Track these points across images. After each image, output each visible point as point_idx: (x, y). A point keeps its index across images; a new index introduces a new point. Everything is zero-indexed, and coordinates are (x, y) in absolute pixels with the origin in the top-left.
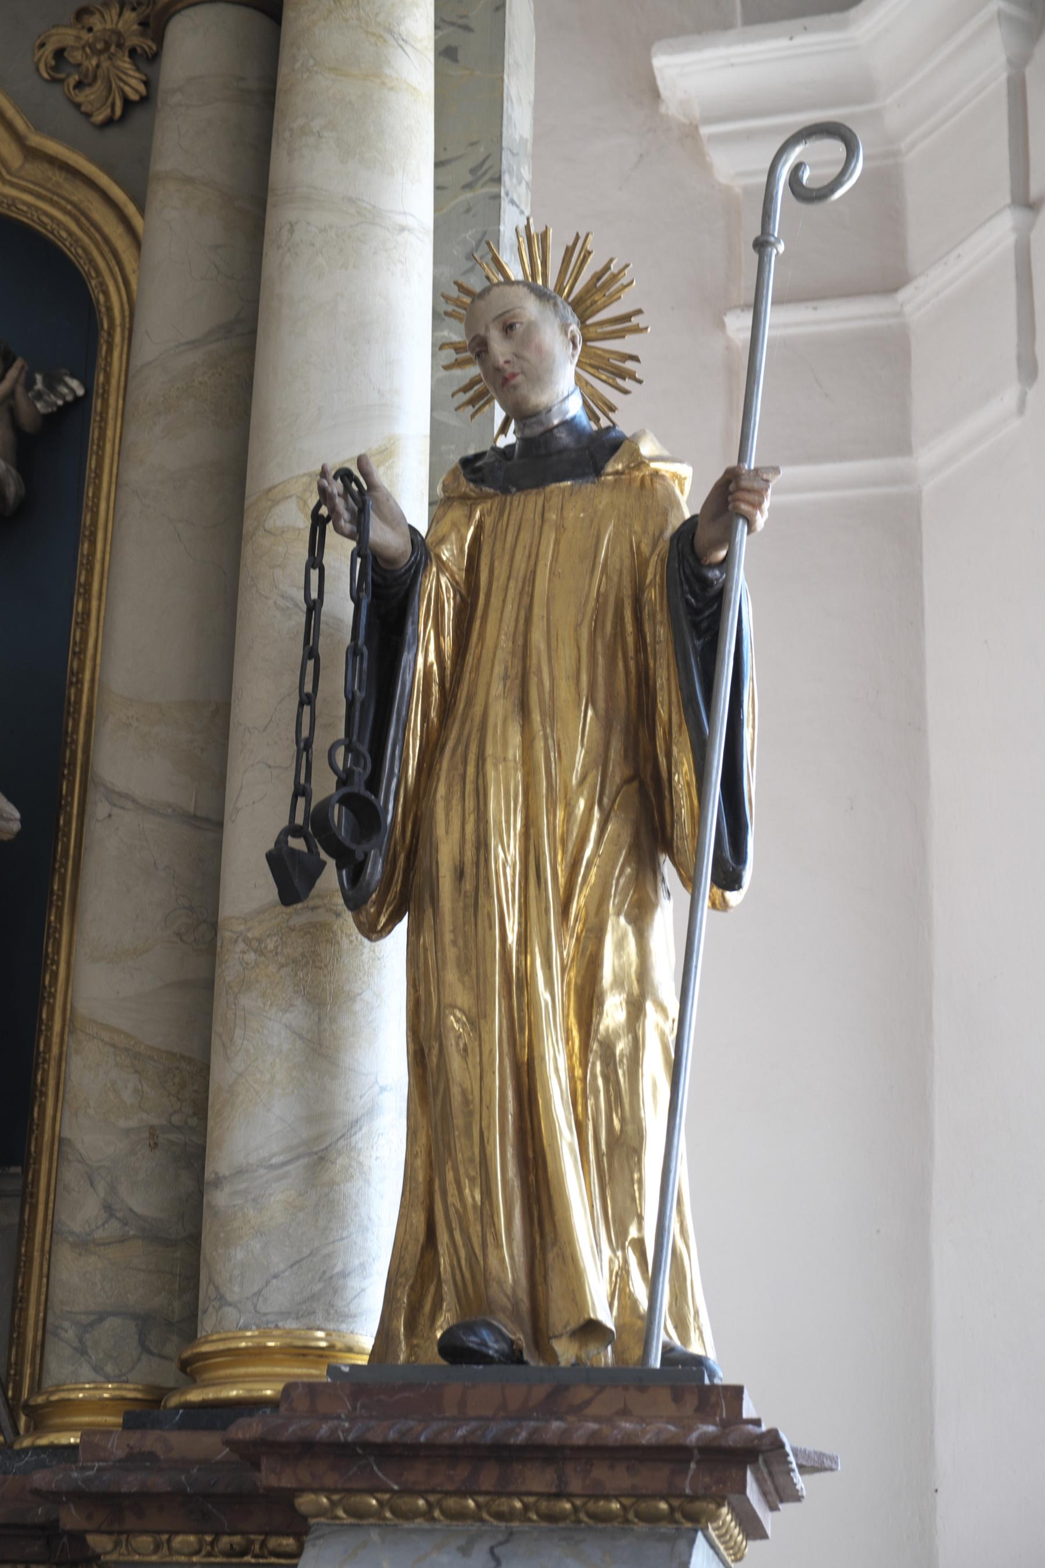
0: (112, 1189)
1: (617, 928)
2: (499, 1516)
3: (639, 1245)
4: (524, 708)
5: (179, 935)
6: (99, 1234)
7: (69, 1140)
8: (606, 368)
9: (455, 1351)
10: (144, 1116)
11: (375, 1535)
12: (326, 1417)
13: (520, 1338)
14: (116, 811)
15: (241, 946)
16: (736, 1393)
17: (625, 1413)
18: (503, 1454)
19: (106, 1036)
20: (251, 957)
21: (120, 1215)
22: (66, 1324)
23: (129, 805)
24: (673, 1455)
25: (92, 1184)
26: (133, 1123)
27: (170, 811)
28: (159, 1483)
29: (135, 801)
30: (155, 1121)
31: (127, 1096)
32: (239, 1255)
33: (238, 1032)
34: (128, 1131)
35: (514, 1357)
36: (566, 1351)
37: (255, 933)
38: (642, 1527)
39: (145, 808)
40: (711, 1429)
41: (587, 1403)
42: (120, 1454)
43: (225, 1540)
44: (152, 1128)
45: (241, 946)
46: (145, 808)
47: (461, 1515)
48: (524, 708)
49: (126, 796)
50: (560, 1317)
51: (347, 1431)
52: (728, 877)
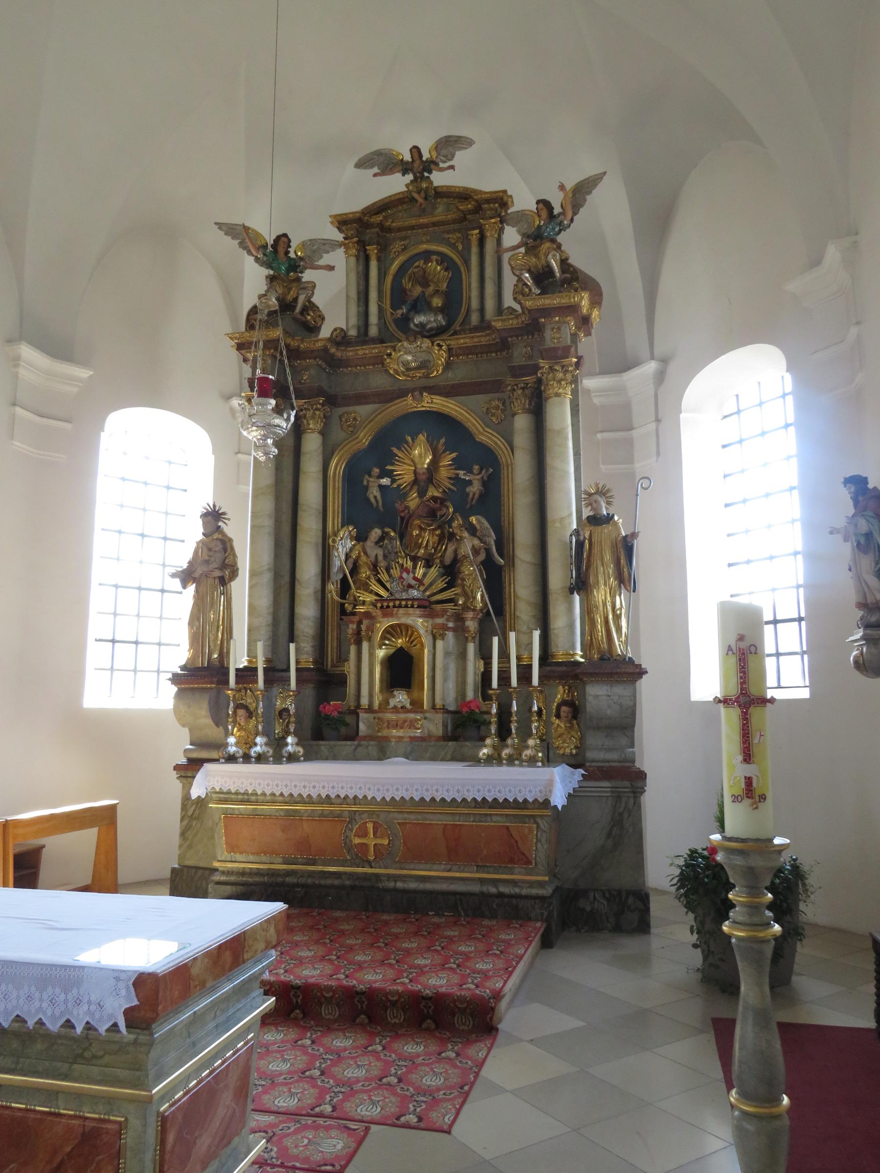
1: (618, 598)
4: (603, 564)
8: (609, 503)
18: (611, 673)
24: (633, 673)
35: (609, 659)
46: (528, 563)
48: (603, 564)
50: (614, 654)
51: (592, 671)
52: (634, 591)
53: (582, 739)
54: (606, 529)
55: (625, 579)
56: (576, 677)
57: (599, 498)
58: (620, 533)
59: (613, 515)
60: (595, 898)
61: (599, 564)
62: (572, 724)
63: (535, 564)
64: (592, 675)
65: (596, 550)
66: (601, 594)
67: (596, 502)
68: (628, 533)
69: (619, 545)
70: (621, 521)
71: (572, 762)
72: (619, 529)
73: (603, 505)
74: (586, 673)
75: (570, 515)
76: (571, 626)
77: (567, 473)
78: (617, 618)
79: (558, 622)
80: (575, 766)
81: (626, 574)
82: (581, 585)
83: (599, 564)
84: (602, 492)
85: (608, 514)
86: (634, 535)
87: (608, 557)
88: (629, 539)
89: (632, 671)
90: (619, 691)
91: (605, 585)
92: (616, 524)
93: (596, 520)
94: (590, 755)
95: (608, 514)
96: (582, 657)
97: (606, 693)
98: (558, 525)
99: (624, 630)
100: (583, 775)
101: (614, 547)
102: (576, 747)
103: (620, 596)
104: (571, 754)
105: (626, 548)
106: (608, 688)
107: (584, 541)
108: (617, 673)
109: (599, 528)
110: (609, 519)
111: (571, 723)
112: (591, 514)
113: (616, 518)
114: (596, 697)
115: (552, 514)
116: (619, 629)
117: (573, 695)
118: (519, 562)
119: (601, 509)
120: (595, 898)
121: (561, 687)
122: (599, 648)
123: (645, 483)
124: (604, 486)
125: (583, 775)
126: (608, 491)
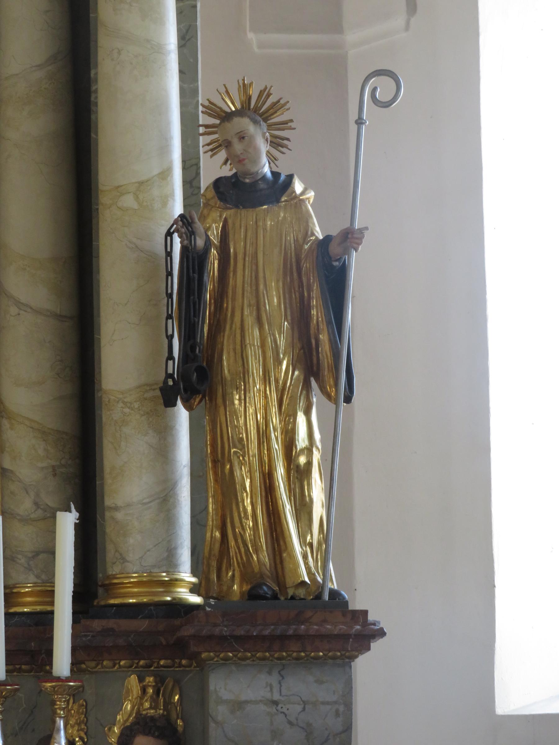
0: (37, 495)
2: (279, 659)
3: (311, 545)
5: (58, 374)
6: (33, 516)
7: (12, 472)
10: (50, 461)
11: (233, 668)
12: (215, 625)
13: (276, 588)
14: (22, 312)
15: (121, 405)
16: (365, 613)
17: (325, 621)
18: (283, 639)
19: (27, 423)
20: (127, 410)
21: (42, 507)
22: (20, 556)
23: (29, 310)
24: (344, 637)
25: (27, 493)
26: (44, 464)
27: (49, 313)
28: (121, 642)
29: (31, 308)
30: (53, 463)
31: (41, 452)
32: (131, 541)
33: (123, 444)
34: (43, 468)
35: (275, 597)
36: (291, 592)
37: (128, 399)
38: (330, 661)
39: (37, 312)
40: (358, 627)
41: (311, 617)
42: (99, 629)
43: (142, 662)
44: (53, 467)
45: (121, 405)
46: (37, 312)
47: (264, 659)
49: (27, 305)
50: (290, 581)
51: (226, 631)
54: (270, 218)
55: (322, 365)
56: (179, 648)
57: (251, 128)
58: (307, 232)
59: (290, 178)
61: (250, 320)
63: (60, 317)
64: (223, 642)
65: (239, 278)
66: (251, 409)
68: (334, 232)
70: (311, 194)
72: (303, 220)
73: (263, 147)
74: (210, 637)
75: (166, 174)
76: (166, 499)
77: (159, 49)
78: (299, 475)
79: (127, 487)
81: (325, 347)
82: (196, 378)
83: (250, 320)
84: (259, 109)
86: (350, 238)
87: (274, 300)
88: (334, 249)
89: (341, 628)
90: (302, 686)
91: (266, 379)
92: (298, 202)
93: (240, 191)
96: (194, 589)
97: (264, 693)
98: (128, 201)
99: (318, 511)
101: (293, 269)
103: (308, 413)
105: (325, 274)
106: (274, 679)
108: (298, 637)
109: (248, 216)
110: (278, 188)
112: (227, 171)
113: (298, 187)
114: (238, 706)
115: (111, 172)
116: (303, 508)
117: (168, 703)
118: (13, 310)
119: (256, 160)
121: (133, 679)
123: (384, 88)
124: (265, 94)
126: (277, 107)
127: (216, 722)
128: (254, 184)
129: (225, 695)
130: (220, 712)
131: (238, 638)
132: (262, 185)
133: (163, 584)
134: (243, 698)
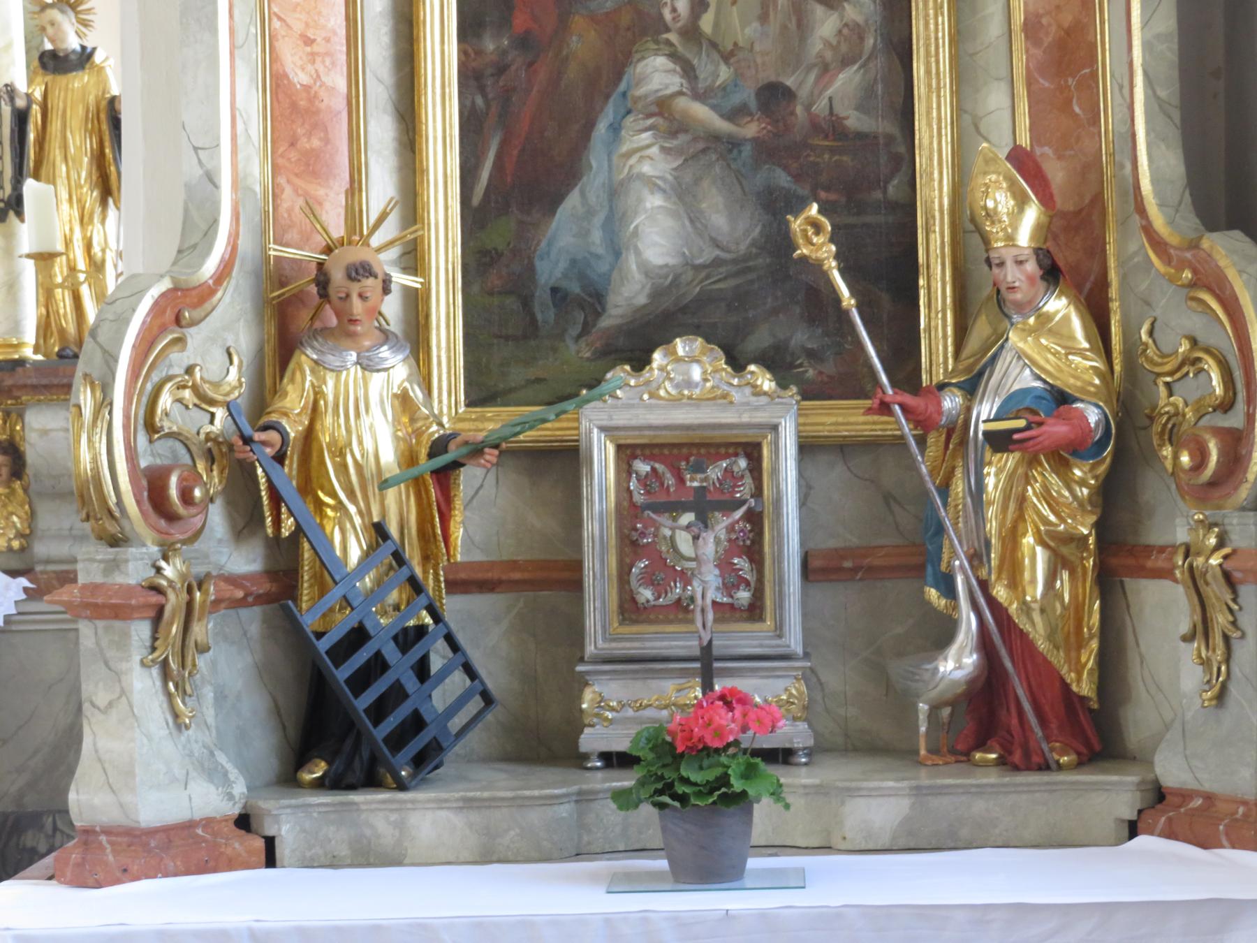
9: (60, 355)
12: (30, 377)
53: (32, 515)
54: (79, 81)
60: (55, 829)
61: (59, 159)
62: (13, 492)
64: (35, 388)
65: (55, 126)
67: (53, 24)
69: (103, 116)
71: (15, 564)
74: (25, 386)
80: (13, 573)
83: (59, 159)
85: (83, 48)
92: (101, 69)
94: (41, 549)
95: (83, 48)
100: (26, 590)
102: (20, 535)
103: (103, 222)
104: (10, 549)
107: (28, 108)
109: (62, 80)
110: (84, 58)
111: (9, 487)
113: (98, 58)
114: (45, 433)
117: (13, 430)
120: (55, 829)
122: (62, 332)
125: (26, 590)
127: (31, 444)
128: (67, 56)
129: (36, 425)
130: (32, 437)
131: (46, 387)
132: (73, 57)
133: (11, 346)
134: (48, 427)
